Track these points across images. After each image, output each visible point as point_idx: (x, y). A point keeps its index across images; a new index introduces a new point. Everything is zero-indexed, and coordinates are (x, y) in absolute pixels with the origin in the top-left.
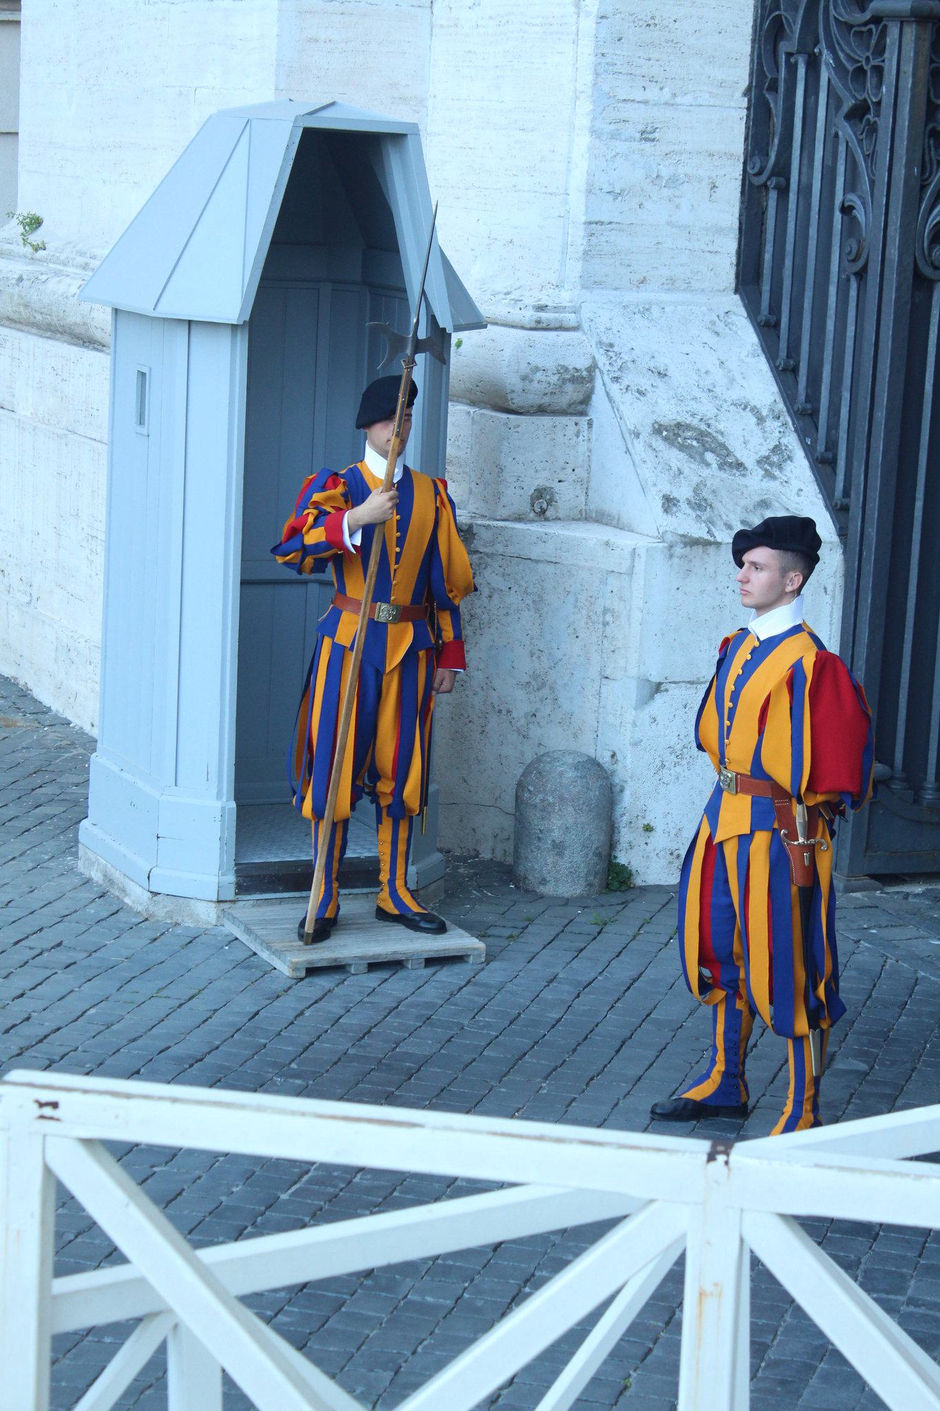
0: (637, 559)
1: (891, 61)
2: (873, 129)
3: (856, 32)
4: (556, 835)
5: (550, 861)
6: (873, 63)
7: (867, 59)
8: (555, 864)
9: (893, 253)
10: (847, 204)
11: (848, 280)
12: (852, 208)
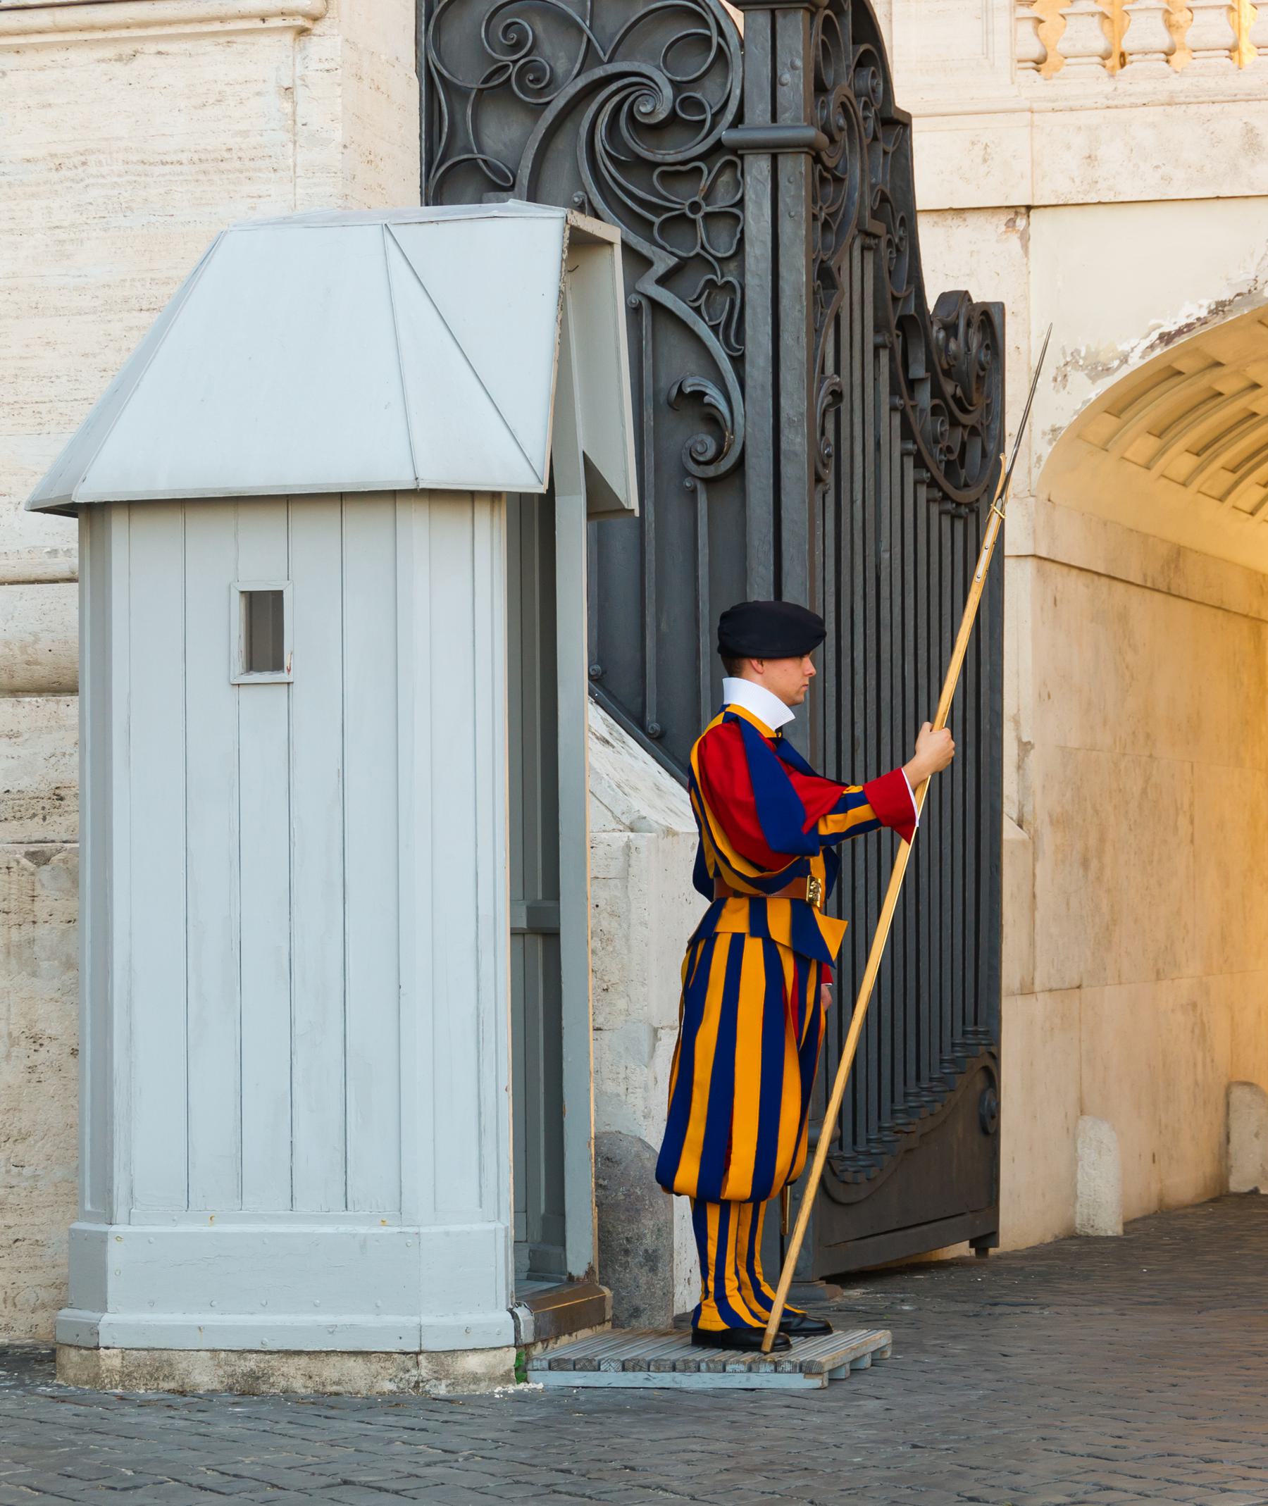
0: (634, 854)
1: (759, 205)
3: (663, 175)
4: (649, 1242)
5: (642, 1281)
8: (650, 1285)
9: (796, 441)
11: (694, 491)
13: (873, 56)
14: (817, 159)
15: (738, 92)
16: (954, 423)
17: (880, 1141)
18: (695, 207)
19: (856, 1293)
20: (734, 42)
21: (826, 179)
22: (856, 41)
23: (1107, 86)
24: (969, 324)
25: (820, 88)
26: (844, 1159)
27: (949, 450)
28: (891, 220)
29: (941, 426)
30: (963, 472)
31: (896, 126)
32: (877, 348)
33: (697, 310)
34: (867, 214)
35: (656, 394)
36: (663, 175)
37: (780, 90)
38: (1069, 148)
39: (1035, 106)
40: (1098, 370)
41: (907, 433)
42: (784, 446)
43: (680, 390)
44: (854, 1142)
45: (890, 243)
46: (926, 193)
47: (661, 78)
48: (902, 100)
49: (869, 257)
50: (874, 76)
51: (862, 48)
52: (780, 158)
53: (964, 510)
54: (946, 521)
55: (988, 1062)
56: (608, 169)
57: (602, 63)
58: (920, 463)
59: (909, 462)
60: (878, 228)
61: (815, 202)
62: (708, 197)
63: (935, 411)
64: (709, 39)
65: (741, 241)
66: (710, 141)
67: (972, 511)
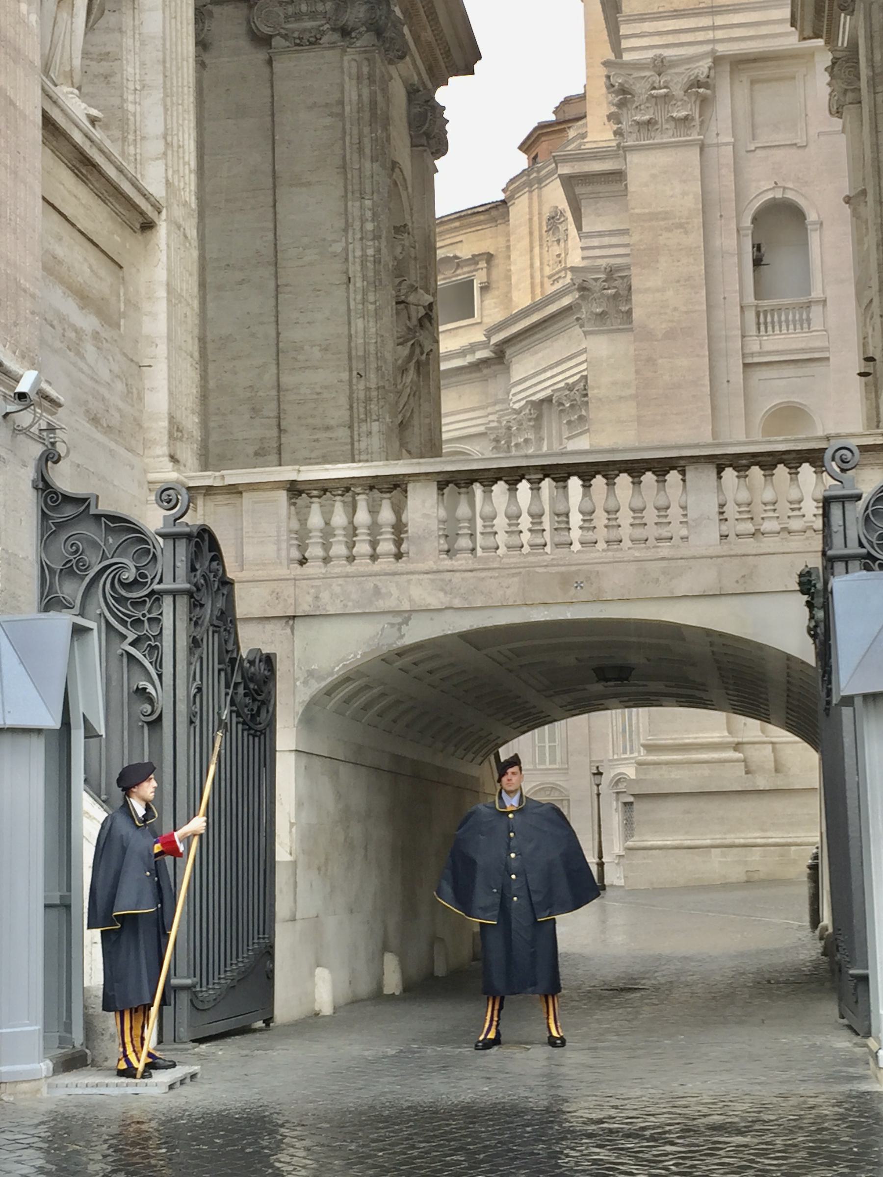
1: (168, 614)
2: (153, 649)
6: (148, 616)
7: (144, 615)
9: (182, 707)
10: (140, 687)
11: (143, 726)
12: (145, 689)
13: (218, 557)
14: (192, 597)
15: (160, 571)
16: (254, 700)
17: (218, 983)
18: (144, 615)
19: (203, 1046)
20: (159, 550)
21: (195, 604)
22: (210, 551)
23: (323, 571)
24: (260, 661)
25: (193, 569)
26: (202, 991)
27: (252, 710)
28: (226, 620)
29: (247, 700)
30: (258, 719)
31: (227, 583)
32: (220, 671)
33: (144, 655)
34: (214, 618)
35: (129, 688)
36: (131, 603)
37: (177, 569)
38: (308, 593)
39: (297, 577)
40: (321, 678)
41: (233, 703)
42: (177, 709)
43: (137, 688)
44: (208, 984)
45: (225, 630)
46: (241, 610)
47: (131, 565)
48: (230, 575)
49: (216, 635)
50: (218, 564)
51: (212, 554)
52: (177, 597)
53: (258, 733)
54: (251, 738)
55: (269, 949)
56: (111, 601)
57: (108, 559)
58: (238, 716)
59: (234, 715)
60: (220, 623)
61: (191, 613)
62: (149, 612)
63: (246, 695)
64: (149, 549)
65: (161, 629)
66: (150, 590)
67: (262, 733)
